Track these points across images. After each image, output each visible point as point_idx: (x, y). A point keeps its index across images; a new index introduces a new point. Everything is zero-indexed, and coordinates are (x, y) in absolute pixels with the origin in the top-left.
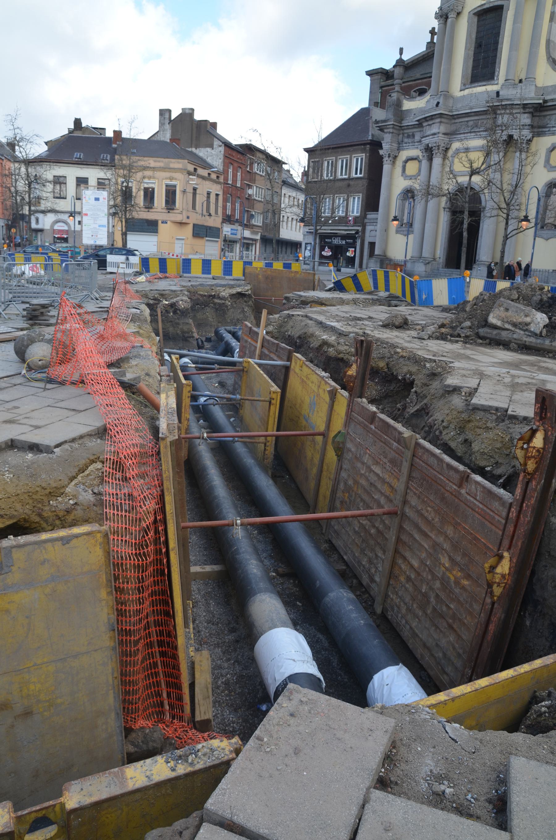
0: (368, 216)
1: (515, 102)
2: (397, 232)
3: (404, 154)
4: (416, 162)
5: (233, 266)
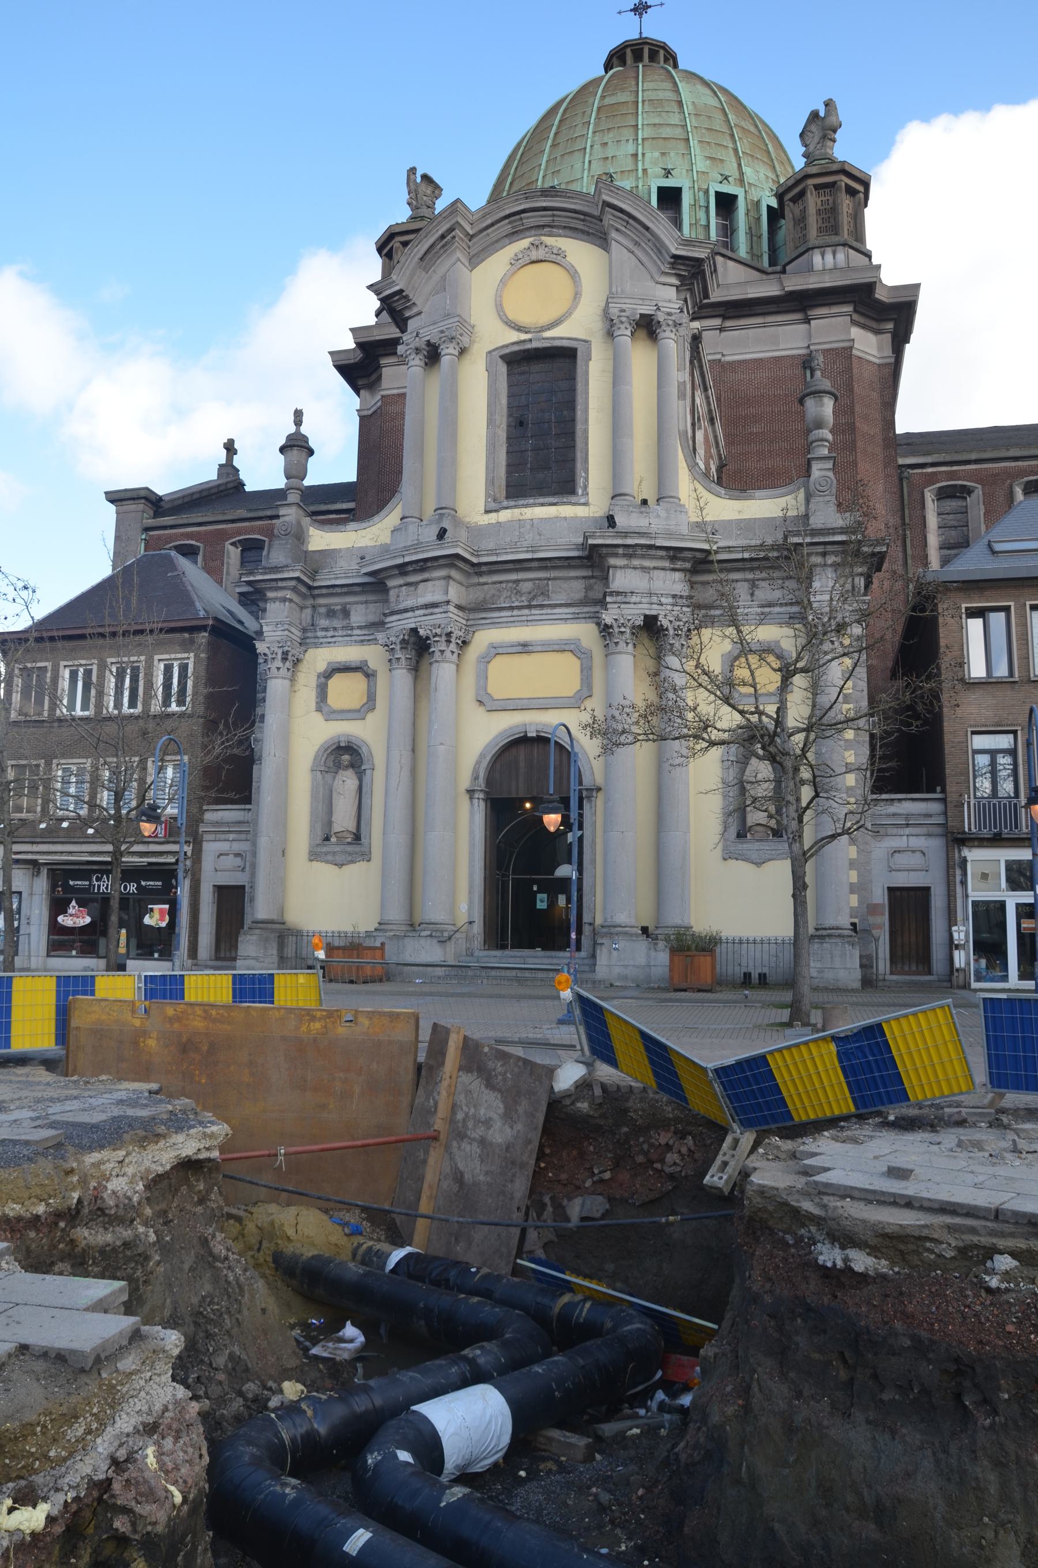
0: (208, 816)
1: (659, 543)
2: (314, 856)
3: (319, 658)
4: (359, 676)
5: (17, 999)
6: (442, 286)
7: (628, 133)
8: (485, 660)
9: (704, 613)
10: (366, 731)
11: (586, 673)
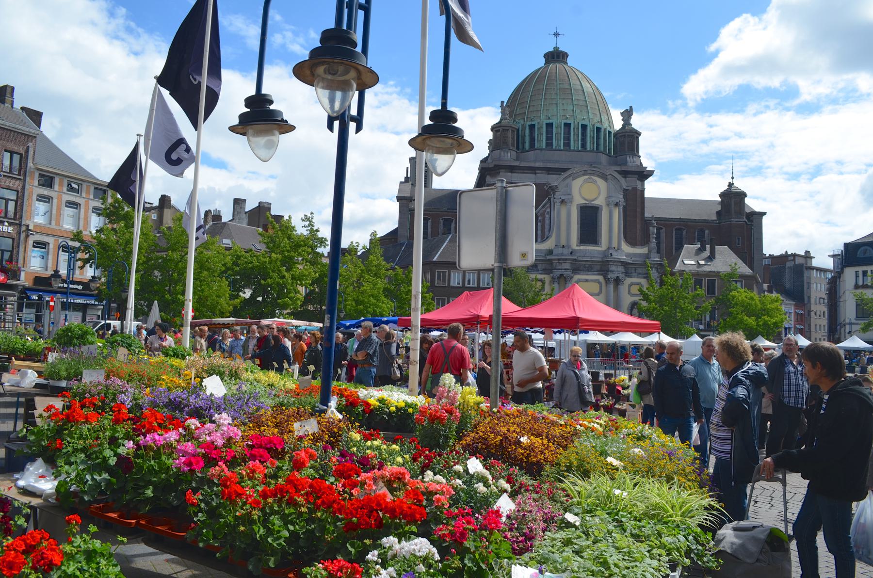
6: (567, 186)
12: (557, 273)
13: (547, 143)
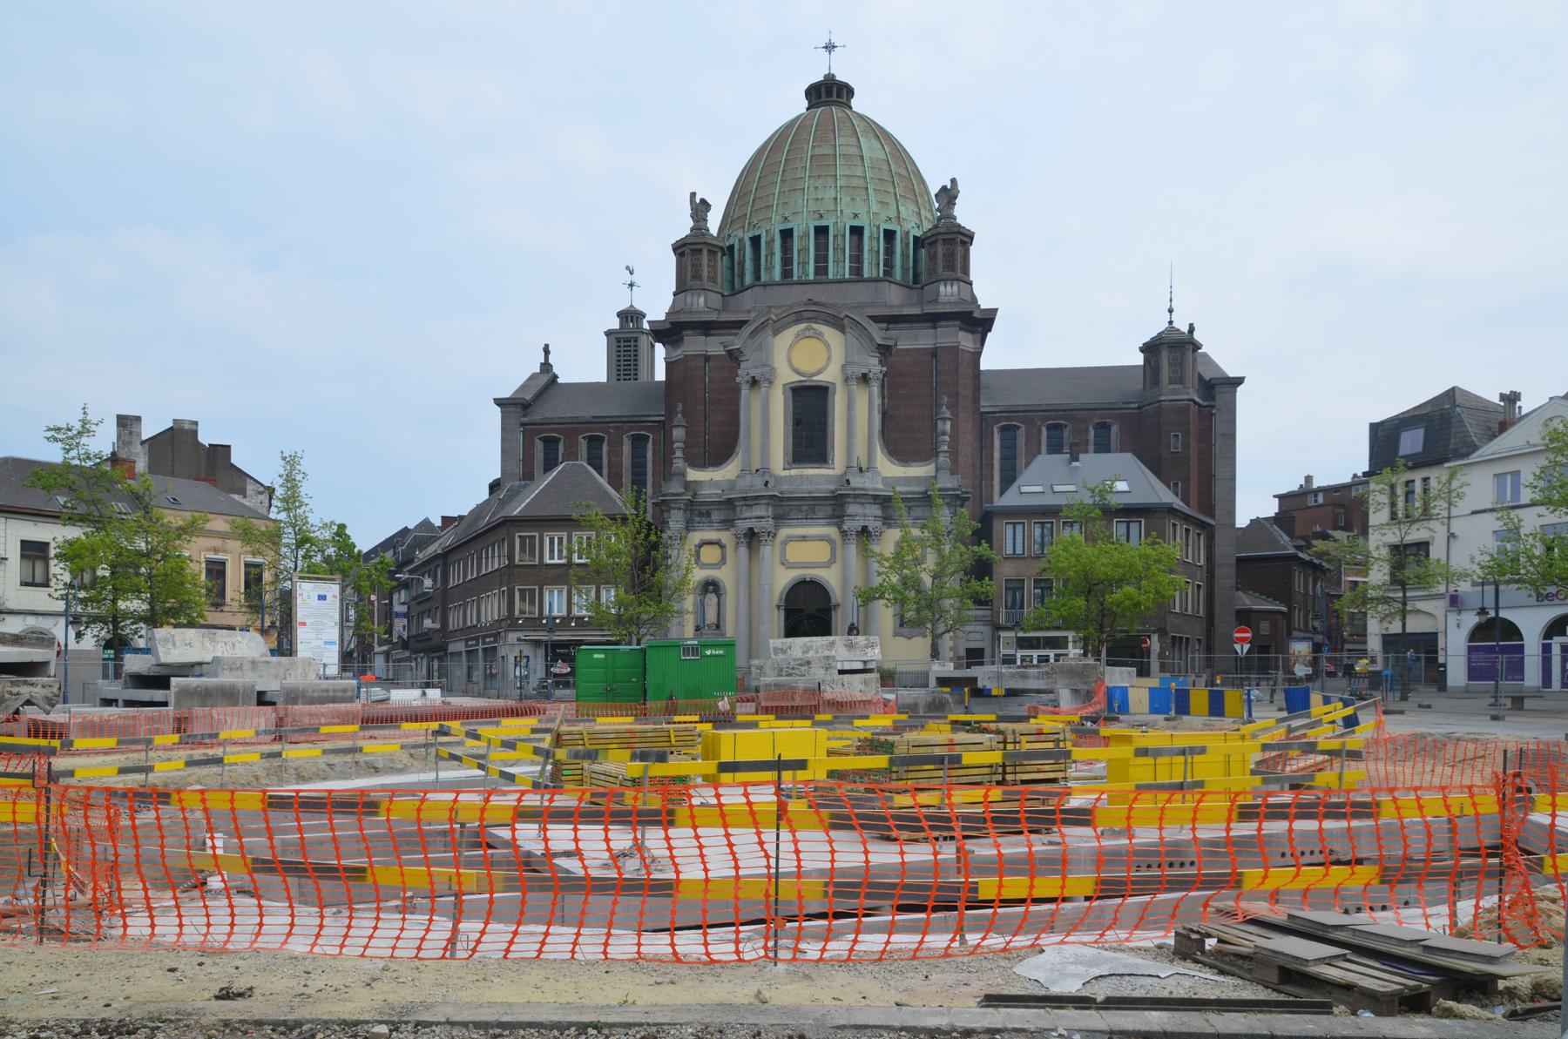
3: (696, 537)
6: (760, 347)
7: (830, 181)
8: (785, 543)
9: (888, 521)
10: (723, 575)
11: (833, 551)
12: (743, 525)
13: (817, 272)
